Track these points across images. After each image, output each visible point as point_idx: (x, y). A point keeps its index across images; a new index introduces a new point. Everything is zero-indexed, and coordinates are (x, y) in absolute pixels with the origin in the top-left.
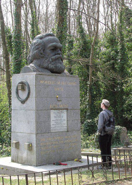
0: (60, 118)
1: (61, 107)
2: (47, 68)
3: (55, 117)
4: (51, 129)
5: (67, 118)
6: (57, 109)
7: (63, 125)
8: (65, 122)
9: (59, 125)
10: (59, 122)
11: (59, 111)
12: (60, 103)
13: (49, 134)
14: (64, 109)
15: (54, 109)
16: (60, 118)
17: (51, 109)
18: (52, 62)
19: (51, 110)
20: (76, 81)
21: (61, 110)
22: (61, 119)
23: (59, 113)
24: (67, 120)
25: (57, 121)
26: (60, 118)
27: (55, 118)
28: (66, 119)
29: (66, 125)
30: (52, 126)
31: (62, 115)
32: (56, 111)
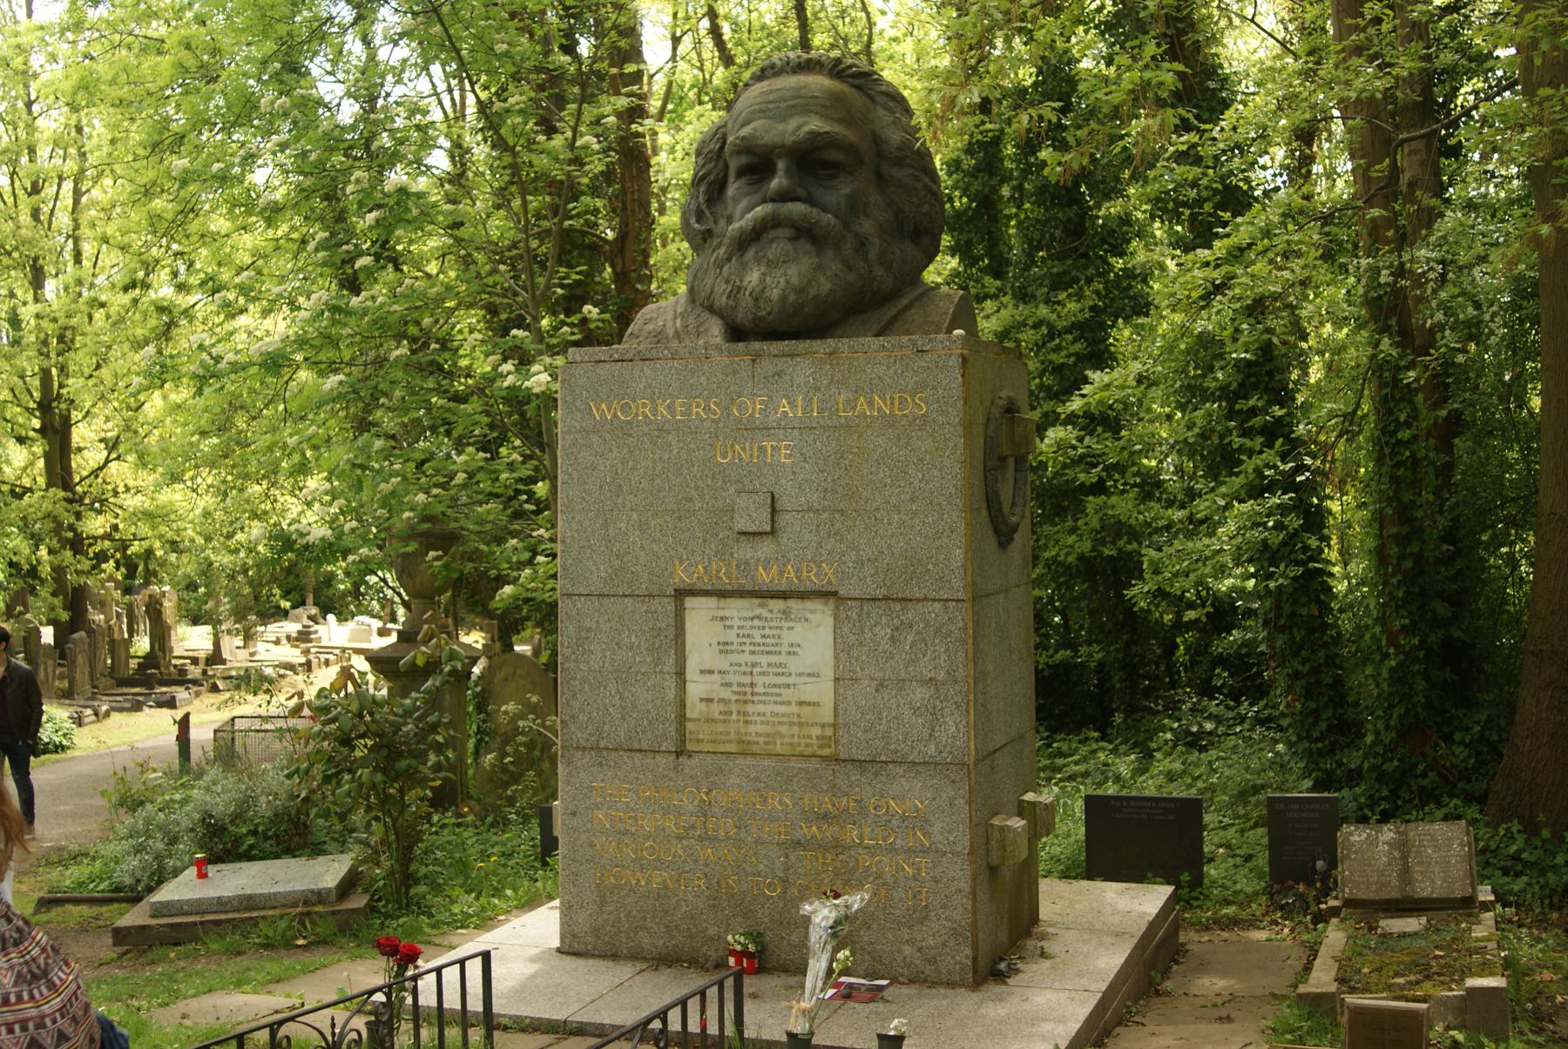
0: (774, 659)
1: (764, 578)
2: (711, 309)
3: (724, 648)
4: (689, 726)
5: (836, 668)
6: (741, 594)
7: (795, 709)
8: (822, 691)
9: (760, 708)
10: (759, 689)
11: (762, 606)
12: (765, 548)
13: (659, 759)
14: (803, 596)
15: (722, 594)
16: (764, 659)
17: (681, 594)
18: (729, 259)
19: (689, 602)
20: (923, 386)
21: (777, 605)
22: (780, 665)
23: (756, 623)
24: (837, 680)
25: (747, 679)
26: (774, 659)
27: (733, 658)
28: (828, 673)
29: (827, 714)
30: (694, 710)
31: (788, 637)
32: (737, 609)
